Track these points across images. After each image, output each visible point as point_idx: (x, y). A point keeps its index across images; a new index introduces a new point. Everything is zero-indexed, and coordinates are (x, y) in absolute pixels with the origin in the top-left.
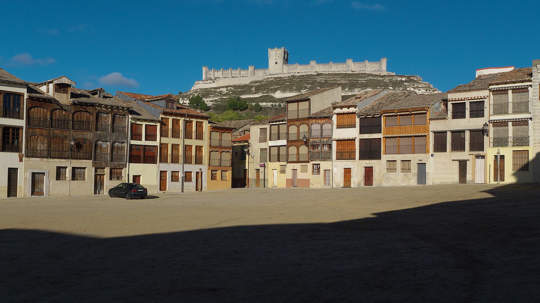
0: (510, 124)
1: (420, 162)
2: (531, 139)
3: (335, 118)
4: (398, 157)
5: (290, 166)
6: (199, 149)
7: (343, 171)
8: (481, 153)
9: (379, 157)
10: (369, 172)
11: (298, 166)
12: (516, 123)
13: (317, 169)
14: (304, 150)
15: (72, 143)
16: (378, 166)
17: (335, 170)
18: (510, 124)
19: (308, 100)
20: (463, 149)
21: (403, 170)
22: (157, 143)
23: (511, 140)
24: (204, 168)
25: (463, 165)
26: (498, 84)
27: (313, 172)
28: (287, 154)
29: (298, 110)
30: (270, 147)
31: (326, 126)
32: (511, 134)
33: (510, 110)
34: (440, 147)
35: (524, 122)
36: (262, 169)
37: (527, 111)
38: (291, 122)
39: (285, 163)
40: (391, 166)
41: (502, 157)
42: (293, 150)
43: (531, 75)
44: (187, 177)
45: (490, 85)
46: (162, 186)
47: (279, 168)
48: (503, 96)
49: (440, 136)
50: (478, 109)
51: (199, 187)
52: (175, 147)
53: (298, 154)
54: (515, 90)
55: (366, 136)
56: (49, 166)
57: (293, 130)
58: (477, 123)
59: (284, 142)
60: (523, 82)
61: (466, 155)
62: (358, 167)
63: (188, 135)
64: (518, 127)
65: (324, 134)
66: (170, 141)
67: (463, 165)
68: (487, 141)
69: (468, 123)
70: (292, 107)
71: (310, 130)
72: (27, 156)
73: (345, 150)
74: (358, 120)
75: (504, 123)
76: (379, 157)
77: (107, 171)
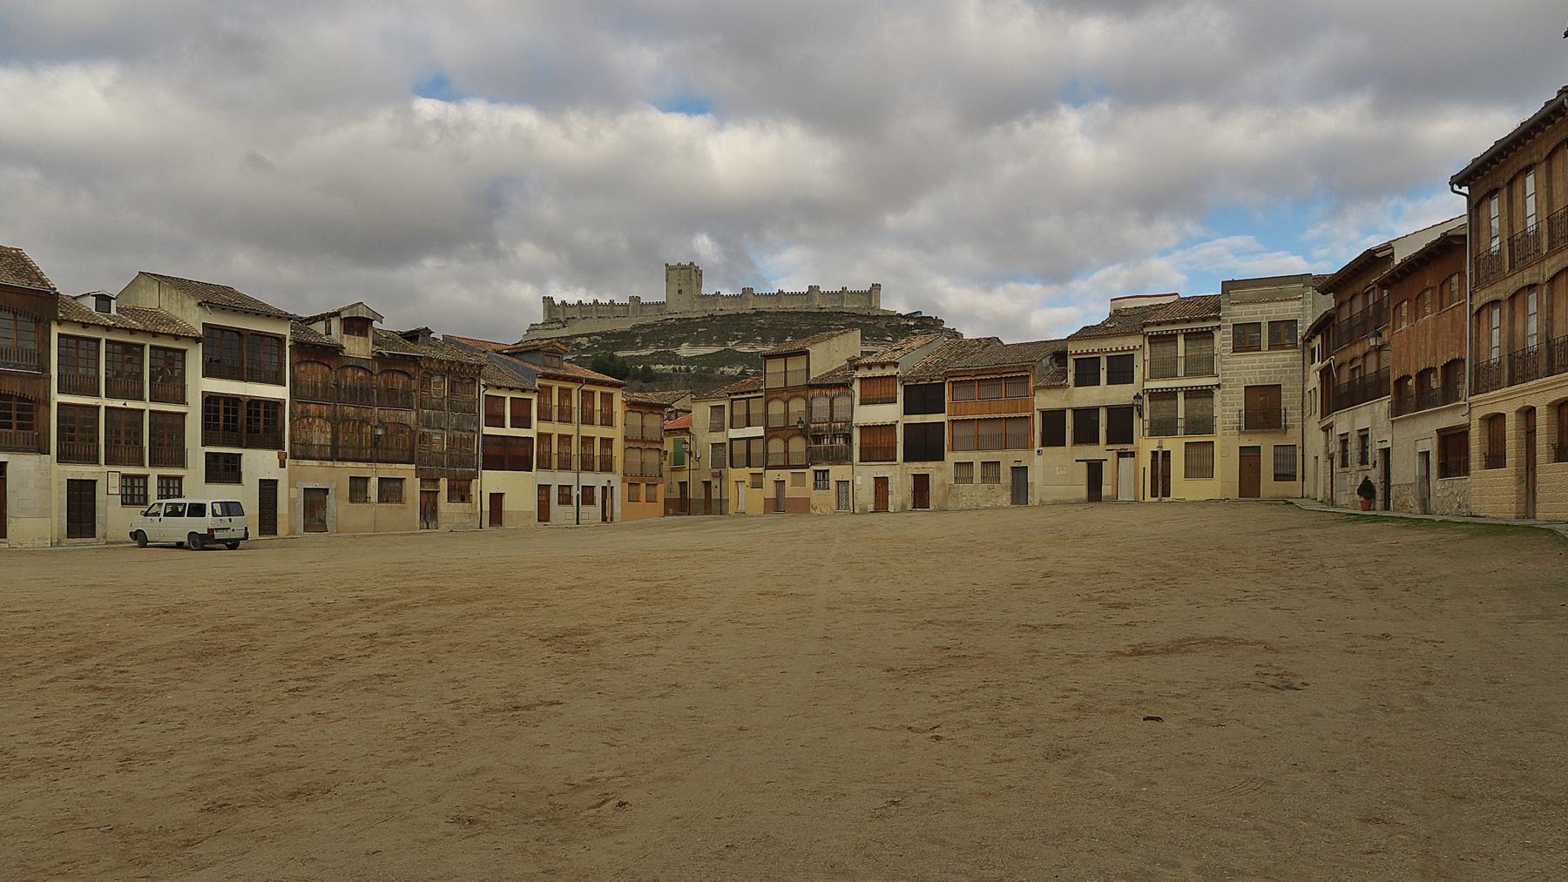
0: (1181, 396)
2: (1218, 423)
3: (856, 387)
4: (977, 457)
5: (772, 475)
6: (607, 443)
7: (872, 483)
8: (1129, 448)
10: (921, 482)
11: (785, 475)
12: (1191, 393)
13: (821, 479)
14: (798, 445)
15: (380, 432)
16: (940, 473)
17: (858, 481)
18: (1181, 396)
19: (807, 353)
20: (1096, 441)
21: (984, 479)
22: (530, 433)
23: (1180, 423)
24: (616, 479)
25: (1095, 469)
26: (1159, 324)
28: (766, 454)
30: (731, 440)
32: (1181, 414)
33: (1181, 372)
34: (1053, 437)
35: (1207, 392)
36: (716, 482)
37: (1211, 374)
38: (771, 395)
39: (761, 470)
41: (1167, 454)
42: (776, 446)
43: (1219, 309)
45: (1145, 325)
46: (544, 514)
47: (748, 480)
48: (1169, 347)
49: (1053, 420)
50: (1121, 370)
51: (608, 514)
53: (787, 452)
54: (1189, 336)
55: (916, 419)
57: (776, 408)
58: (1121, 394)
59: (759, 431)
60: (1204, 320)
61: (1100, 451)
62: (900, 475)
63: (588, 419)
64: (1194, 401)
66: (555, 428)
67: (1095, 469)
68: (1138, 426)
69: (1103, 394)
70: (774, 367)
71: (809, 407)
72: (293, 457)
73: (877, 444)
75: (1171, 394)
77: (443, 483)
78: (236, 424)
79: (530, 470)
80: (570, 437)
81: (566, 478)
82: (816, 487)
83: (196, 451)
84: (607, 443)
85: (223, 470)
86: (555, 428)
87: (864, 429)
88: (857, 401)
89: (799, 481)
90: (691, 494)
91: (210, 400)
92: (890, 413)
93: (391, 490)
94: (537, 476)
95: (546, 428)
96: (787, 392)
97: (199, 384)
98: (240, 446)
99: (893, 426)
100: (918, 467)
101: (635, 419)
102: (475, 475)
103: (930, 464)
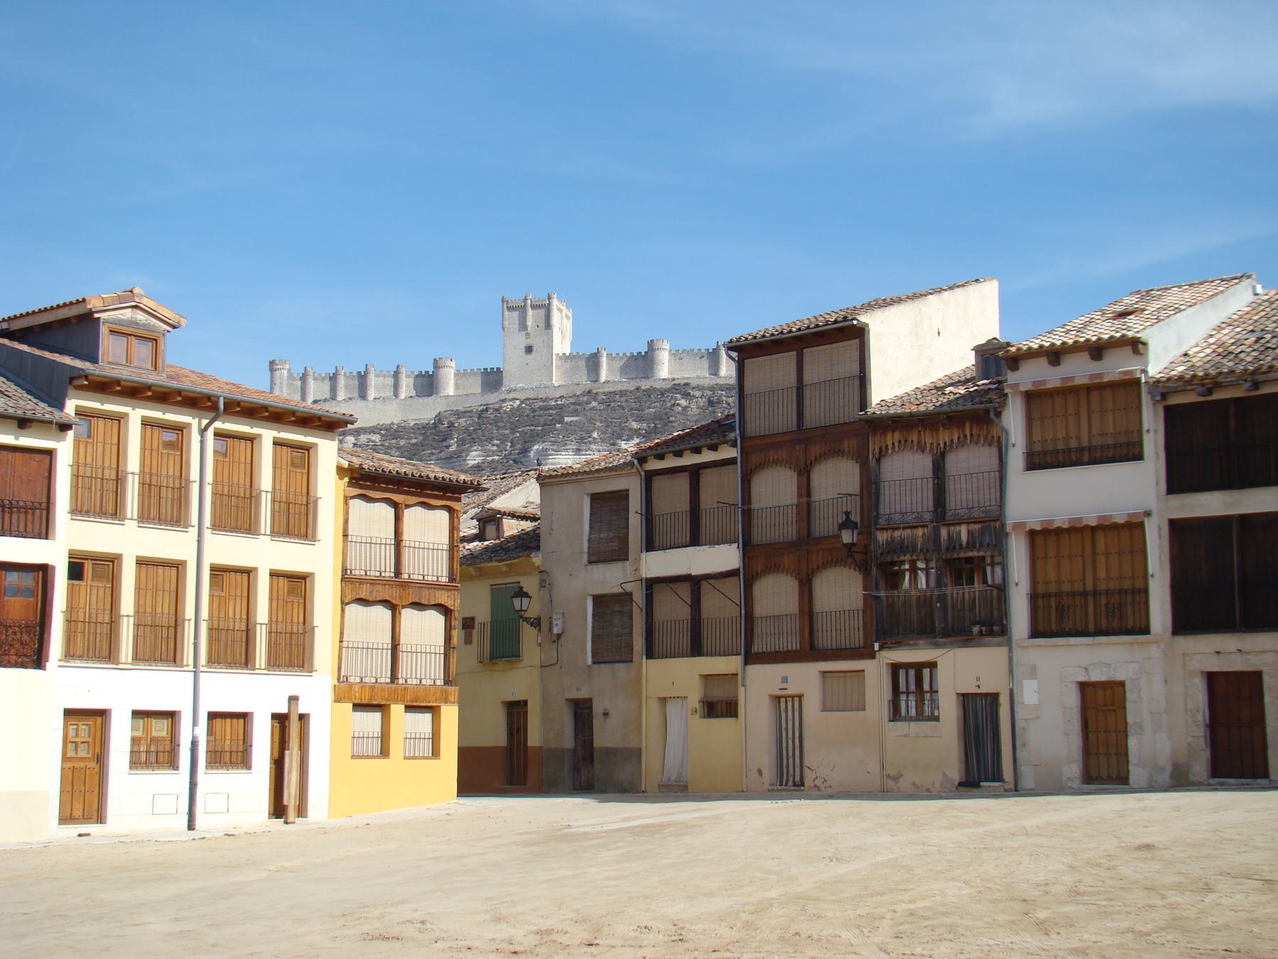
3: (1013, 420)
5: (762, 683)
6: (295, 585)
11: (804, 678)
13: (912, 690)
14: (840, 591)
17: (1029, 693)
19: (857, 334)
22: (51, 552)
24: (314, 692)
31: (968, 462)
39: (731, 664)
42: (776, 595)
44: (229, 738)
57: (776, 489)
59: (726, 557)
63: (235, 514)
65: (958, 498)
66: (129, 540)
71: (871, 487)
79: (37, 660)
80: (178, 566)
81: (163, 687)
82: (895, 715)
84: (295, 585)
86: (129, 540)
87: (1043, 539)
88: (1016, 458)
89: (843, 697)
90: (534, 738)
92: (1131, 488)
95: (96, 536)
99: (1134, 527)
101: (374, 518)
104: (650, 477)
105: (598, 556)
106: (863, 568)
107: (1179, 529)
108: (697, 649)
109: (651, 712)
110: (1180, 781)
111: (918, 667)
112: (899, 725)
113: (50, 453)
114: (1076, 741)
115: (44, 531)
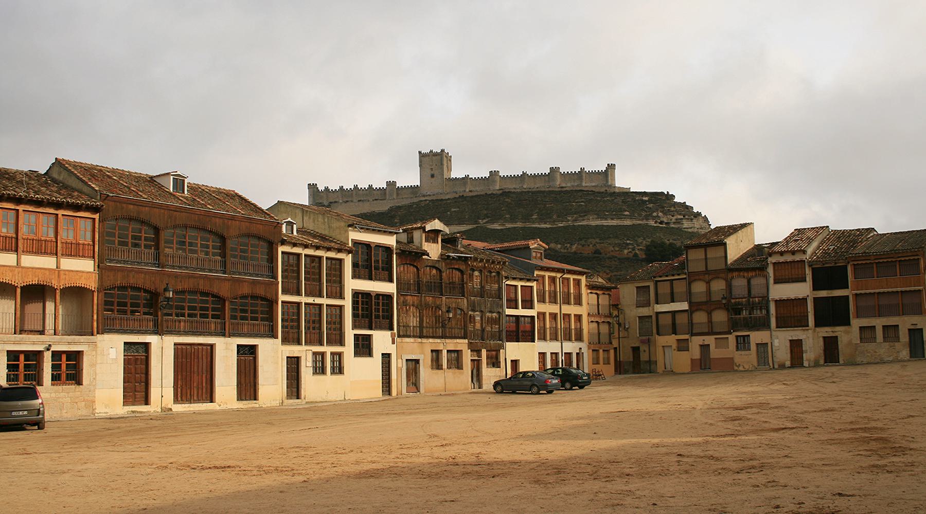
1: (912, 327)
4: (879, 323)
5: (697, 341)
6: (579, 318)
7: (788, 344)
9: (847, 323)
11: (710, 340)
14: (720, 317)
16: (848, 336)
17: (776, 343)
19: (725, 244)
21: (885, 339)
24: (584, 346)
27: (737, 346)
28: (691, 324)
29: (706, 259)
30: (658, 313)
31: (757, 282)
36: (643, 348)
38: (692, 278)
40: (867, 333)
42: (700, 317)
47: (674, 346)
52: (554, 316)
53: (710, 321)
55: (823, 294)
56: (421, 349)
57: (699, 288)
59: (684, 306)
62: (812, 339)
71: (729, 287)
72: (399, 336)
73: (791, 315)
74: (808, 272)
76: (847, 323)
78: (372, 311)
80: (556, 315)
82: (737, 349)
83: (350, 333)
84: (579, 318)
85: (364, 347)
87: (778, 302)
88: (771, 280)
91: (356, 294)
92: (802, 290)
93: (456, 360)
94: (539, 346)
96: (708, 275)
97: (352, 284)
98: (371, 329)
100: (826, 331)
102: (502, 347)
103: (838, 328)
104: (657, 281)
105: (639, 306)
106: (728, 310)
107: (816, 300)
108: (675, 333)
109: (660, 351)
110: (816, 365)
111: (744, 336)
112: (739, 352)
113: (532, 287)
114: (789, 355)
115: (531, 307)
